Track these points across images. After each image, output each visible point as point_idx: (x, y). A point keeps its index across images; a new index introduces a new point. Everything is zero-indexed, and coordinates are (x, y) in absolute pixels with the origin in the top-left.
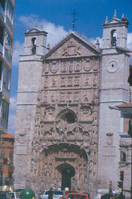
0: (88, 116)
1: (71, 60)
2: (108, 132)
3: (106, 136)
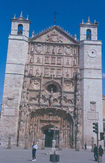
0: (71, 88)
1: (54, 45)
2: (92, 101)
3: (90, 103)
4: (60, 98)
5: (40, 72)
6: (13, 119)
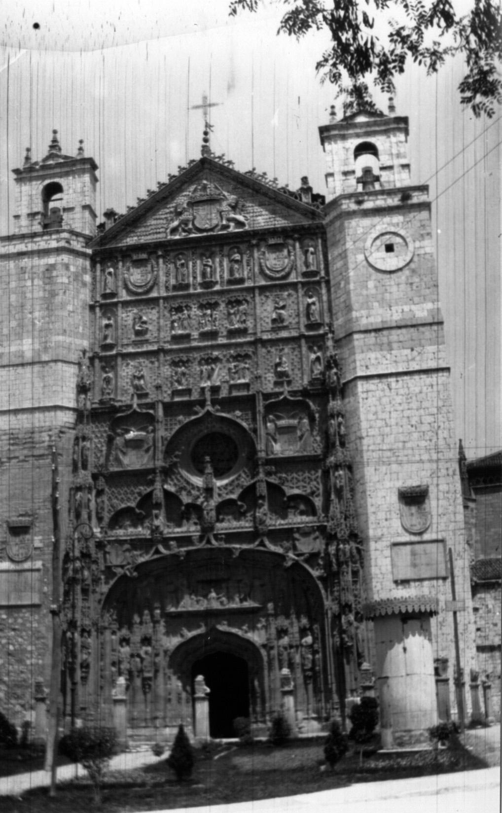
4: (249, 494)
5: (148, 383)
6: (37, 617)
